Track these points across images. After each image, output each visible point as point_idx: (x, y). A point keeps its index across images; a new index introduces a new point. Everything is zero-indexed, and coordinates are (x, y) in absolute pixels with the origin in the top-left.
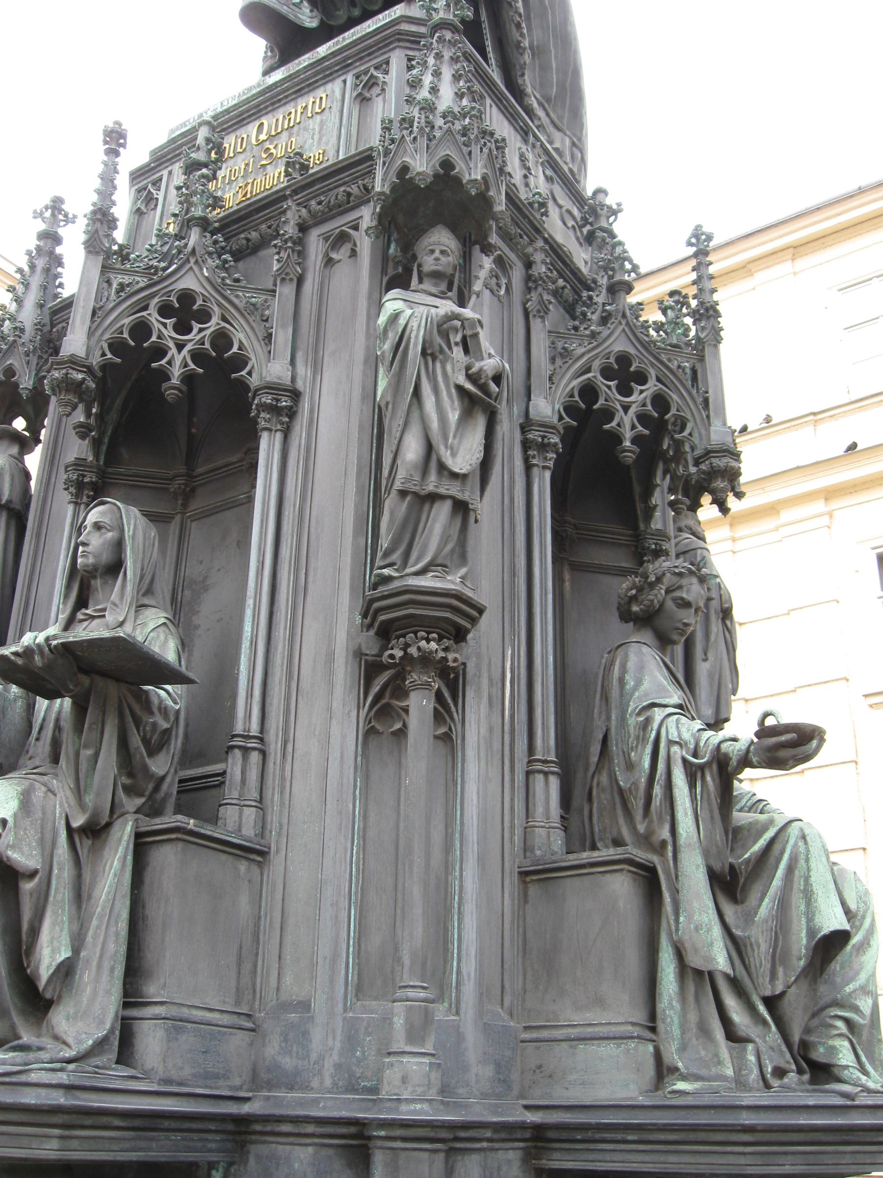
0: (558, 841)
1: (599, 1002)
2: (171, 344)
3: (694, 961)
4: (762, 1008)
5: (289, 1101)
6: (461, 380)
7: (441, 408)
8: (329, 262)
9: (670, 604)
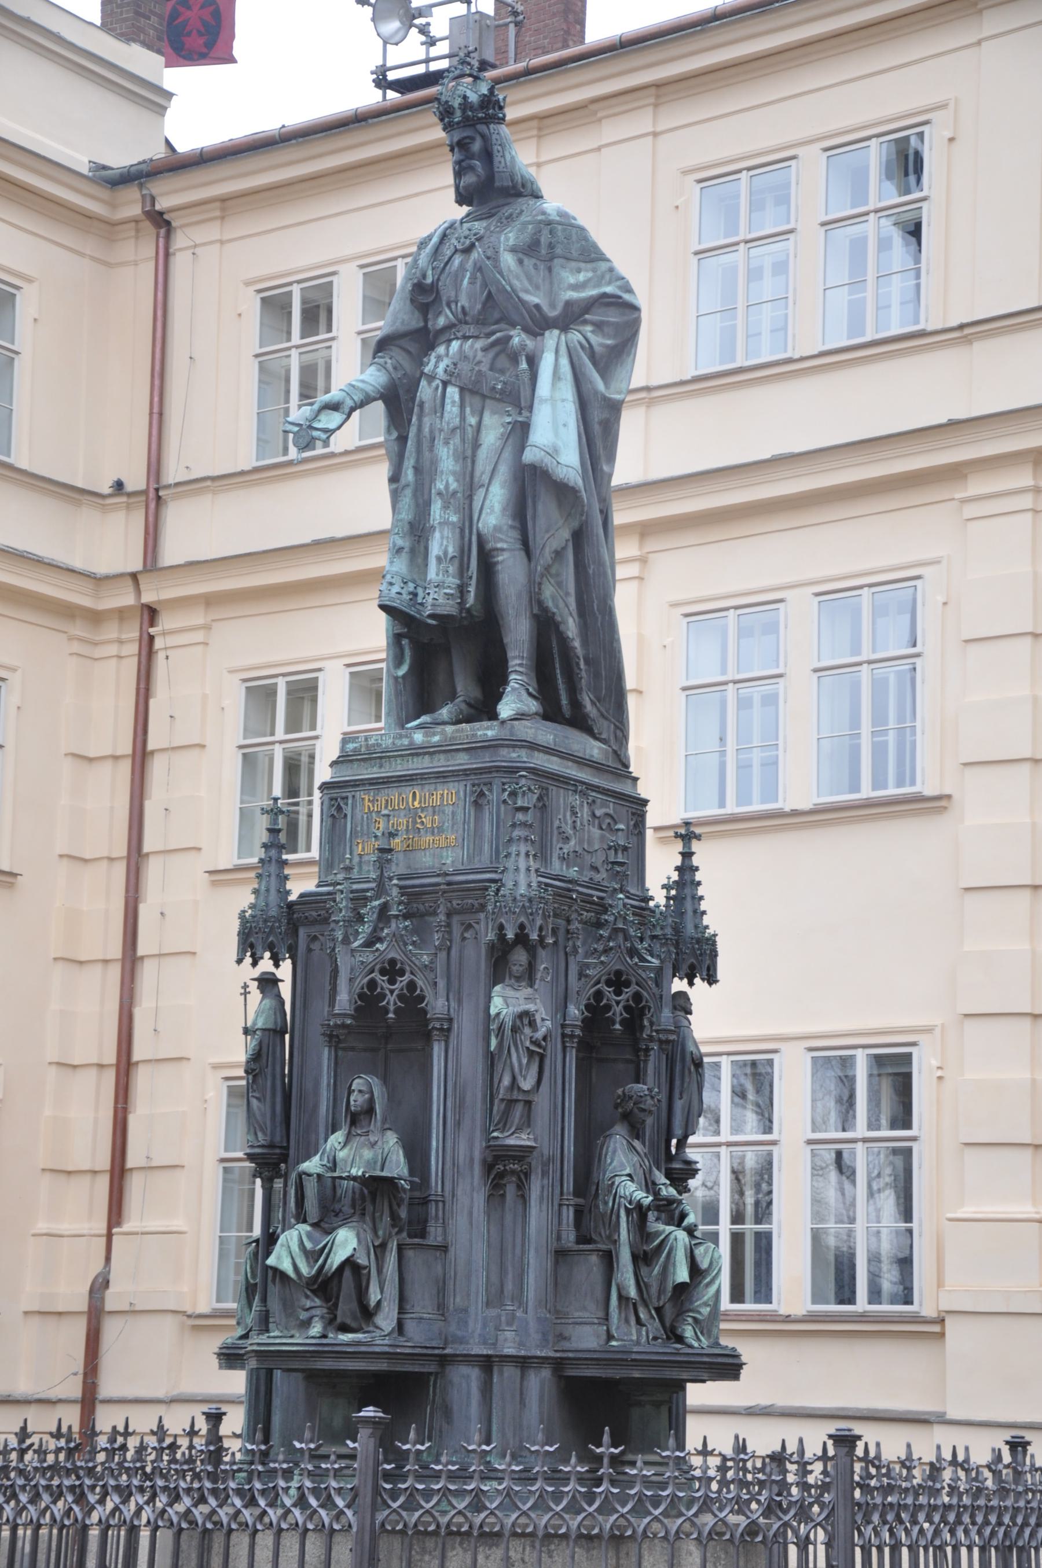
0: (572, 1237)
1: (584, 1308)
2: (388, 992)
3: (624, 1293)
4: (653, 1312)
5: (461, 1349)
6: (528, 1044)
7: (517, 1059)
8: (464, 939)
9: (636, 1110)
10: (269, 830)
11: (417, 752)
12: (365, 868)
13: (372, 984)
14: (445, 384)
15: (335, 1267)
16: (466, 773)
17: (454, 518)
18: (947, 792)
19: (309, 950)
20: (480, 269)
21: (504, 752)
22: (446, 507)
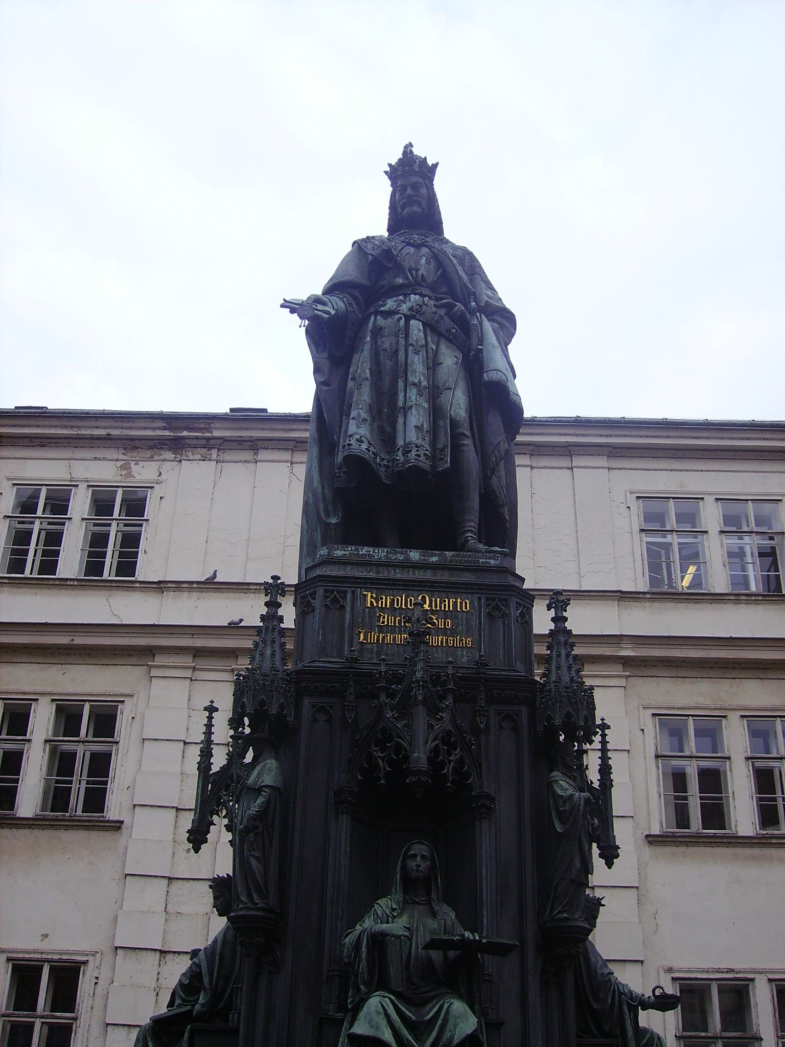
8: (501, 727)
13: (436, 750)
15: (456, 1041)
19: (315, 720)
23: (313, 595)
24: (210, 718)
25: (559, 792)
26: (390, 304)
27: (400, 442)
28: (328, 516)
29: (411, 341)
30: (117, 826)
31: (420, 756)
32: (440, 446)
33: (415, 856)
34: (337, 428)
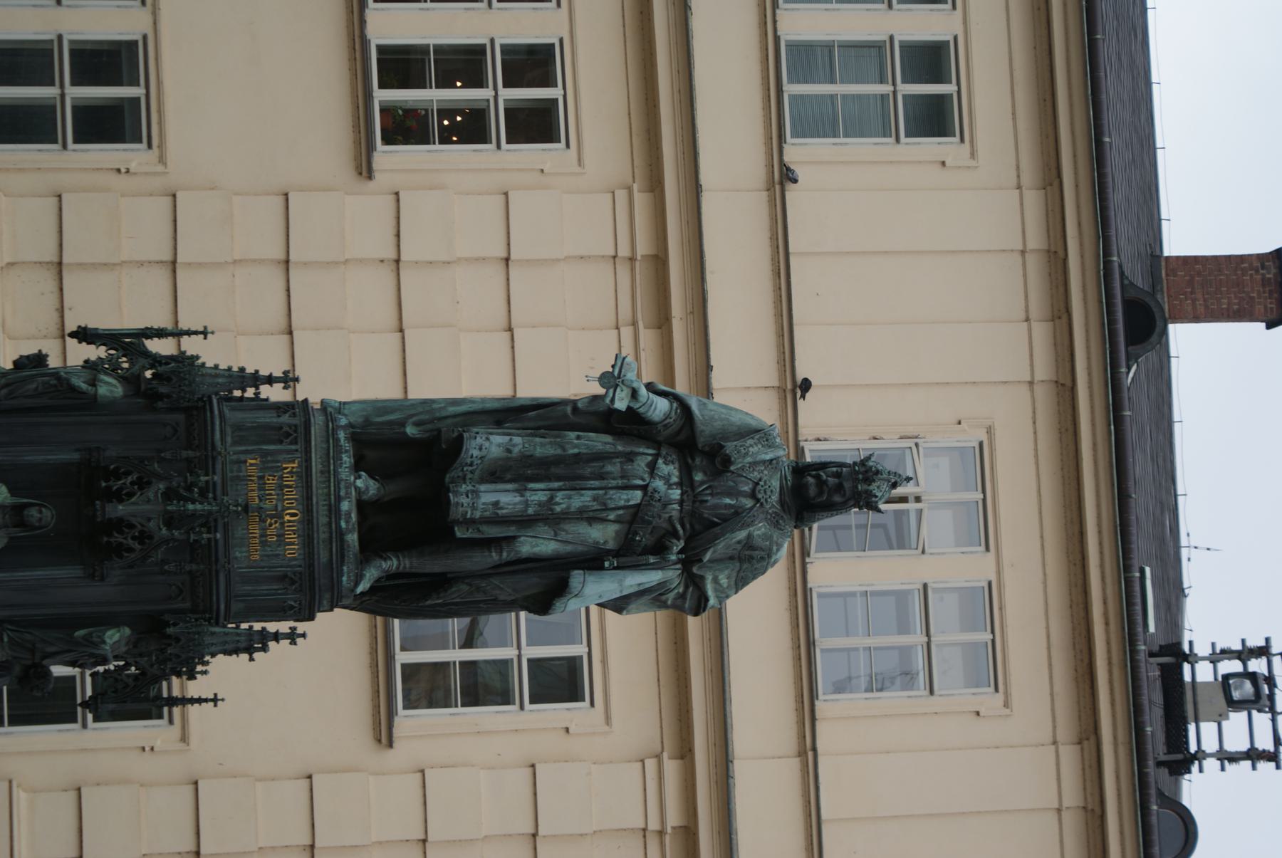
10: (271, 375)
11: (334, 511)
12: (235, 467)
13: (131, 526)
14: (644, 488)
16: (311, 566)
17: (530, 511)
18: (377, 175)
20: (737, 514)
21: (327, 596)
22: (540, 504)
23: (294, 415)
24: (196, 333)
25: (109, 633)
26: (669, 469)
27: (483, 487)
28: (417, 424)
29: (612, 492)
30: (365, 169)
31: (121, 509)
32: (484, 528)
33: (41, 512)
34: (519, 425)
